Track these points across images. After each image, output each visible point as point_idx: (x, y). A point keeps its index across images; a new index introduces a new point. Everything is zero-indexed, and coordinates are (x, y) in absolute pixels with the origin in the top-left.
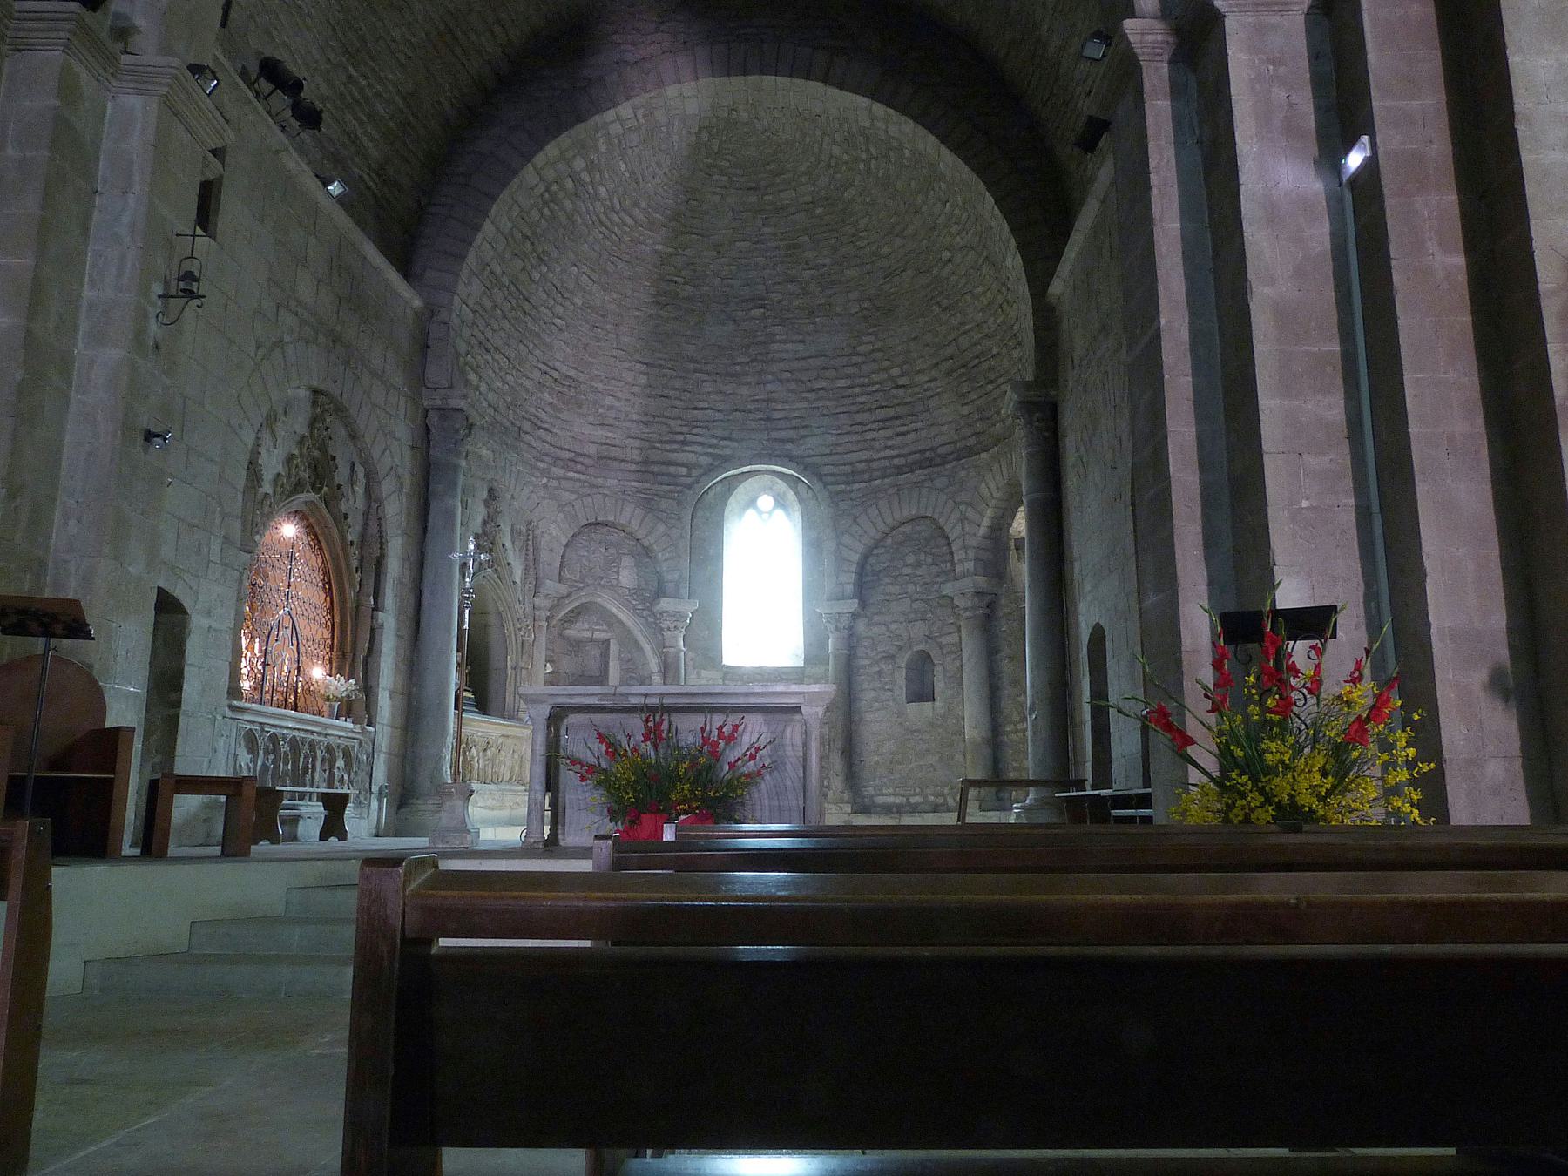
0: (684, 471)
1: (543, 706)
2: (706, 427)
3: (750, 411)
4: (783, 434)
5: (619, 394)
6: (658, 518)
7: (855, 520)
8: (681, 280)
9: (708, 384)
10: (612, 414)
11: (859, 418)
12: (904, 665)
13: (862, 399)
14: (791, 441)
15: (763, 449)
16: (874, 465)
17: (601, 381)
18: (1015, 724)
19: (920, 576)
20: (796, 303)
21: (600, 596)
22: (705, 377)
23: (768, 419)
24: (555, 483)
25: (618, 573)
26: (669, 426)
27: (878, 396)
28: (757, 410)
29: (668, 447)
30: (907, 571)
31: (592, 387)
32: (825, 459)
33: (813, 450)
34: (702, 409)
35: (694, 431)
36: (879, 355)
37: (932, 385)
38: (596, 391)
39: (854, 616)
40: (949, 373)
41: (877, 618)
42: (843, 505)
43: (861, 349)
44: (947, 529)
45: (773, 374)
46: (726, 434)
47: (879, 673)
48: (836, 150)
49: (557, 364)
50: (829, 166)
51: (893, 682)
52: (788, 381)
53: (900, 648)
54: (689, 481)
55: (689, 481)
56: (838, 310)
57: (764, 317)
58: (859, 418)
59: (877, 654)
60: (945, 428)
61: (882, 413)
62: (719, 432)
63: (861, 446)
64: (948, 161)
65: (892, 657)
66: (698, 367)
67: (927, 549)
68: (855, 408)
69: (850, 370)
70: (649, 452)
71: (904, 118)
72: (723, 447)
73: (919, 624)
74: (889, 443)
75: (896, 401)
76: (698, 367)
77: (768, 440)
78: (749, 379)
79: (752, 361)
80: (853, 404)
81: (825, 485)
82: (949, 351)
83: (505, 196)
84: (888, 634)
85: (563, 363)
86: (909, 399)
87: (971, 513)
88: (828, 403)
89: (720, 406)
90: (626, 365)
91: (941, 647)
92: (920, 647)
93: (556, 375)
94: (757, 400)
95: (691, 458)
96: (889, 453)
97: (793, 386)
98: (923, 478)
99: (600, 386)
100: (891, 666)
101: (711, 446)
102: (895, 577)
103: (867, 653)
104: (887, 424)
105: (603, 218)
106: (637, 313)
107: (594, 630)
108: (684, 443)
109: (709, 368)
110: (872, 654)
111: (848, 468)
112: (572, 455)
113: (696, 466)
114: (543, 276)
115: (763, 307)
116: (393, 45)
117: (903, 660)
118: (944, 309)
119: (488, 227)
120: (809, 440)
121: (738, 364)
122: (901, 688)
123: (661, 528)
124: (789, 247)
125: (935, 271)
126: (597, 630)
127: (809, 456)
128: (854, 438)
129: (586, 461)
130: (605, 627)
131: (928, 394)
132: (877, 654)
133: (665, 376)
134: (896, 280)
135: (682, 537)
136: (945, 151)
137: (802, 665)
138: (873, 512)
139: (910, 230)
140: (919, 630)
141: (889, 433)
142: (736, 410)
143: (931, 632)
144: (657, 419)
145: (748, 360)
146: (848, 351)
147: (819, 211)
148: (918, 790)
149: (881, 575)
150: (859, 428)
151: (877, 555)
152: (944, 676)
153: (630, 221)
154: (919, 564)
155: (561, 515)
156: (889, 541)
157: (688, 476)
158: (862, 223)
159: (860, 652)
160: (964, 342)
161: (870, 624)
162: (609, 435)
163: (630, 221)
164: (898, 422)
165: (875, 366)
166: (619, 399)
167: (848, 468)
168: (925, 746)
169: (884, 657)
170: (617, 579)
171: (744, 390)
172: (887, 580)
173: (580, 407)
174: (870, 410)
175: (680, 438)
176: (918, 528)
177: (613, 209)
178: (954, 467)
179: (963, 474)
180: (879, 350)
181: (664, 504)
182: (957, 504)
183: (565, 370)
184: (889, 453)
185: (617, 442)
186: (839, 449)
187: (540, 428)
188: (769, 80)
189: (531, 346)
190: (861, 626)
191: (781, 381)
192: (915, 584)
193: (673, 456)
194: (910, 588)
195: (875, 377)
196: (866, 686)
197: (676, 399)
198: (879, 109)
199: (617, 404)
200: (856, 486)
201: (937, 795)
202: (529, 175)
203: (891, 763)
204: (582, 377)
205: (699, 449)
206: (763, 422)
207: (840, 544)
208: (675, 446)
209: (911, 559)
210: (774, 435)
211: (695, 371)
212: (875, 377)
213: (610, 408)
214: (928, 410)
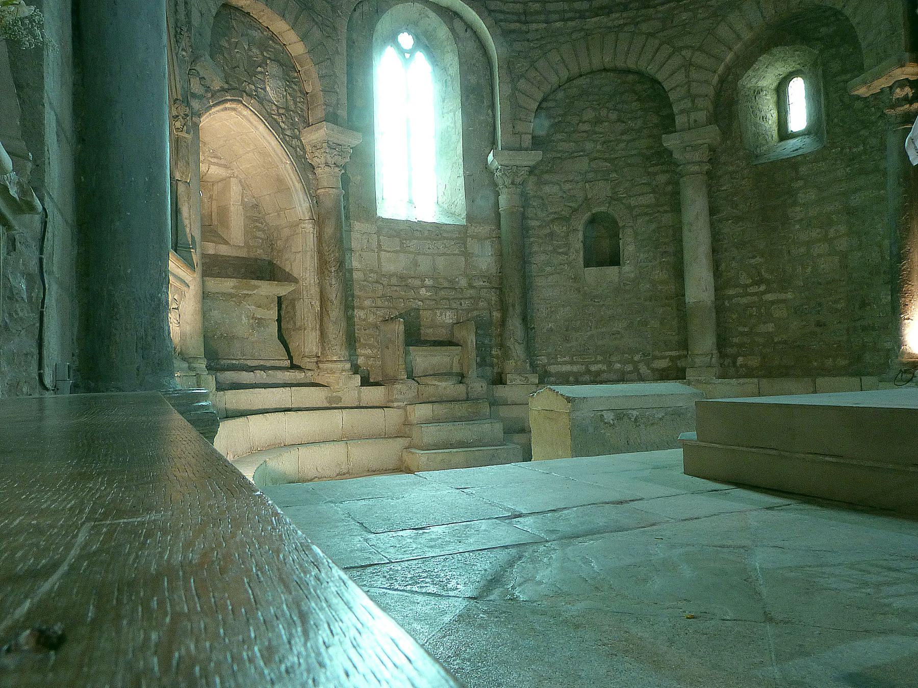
7: (532, 64)
19: (601, 133)
30: (586, 127)
41: (546, 177)
47: (552, 235)
51: (568, 245)
53: (575, 210)
59: (548, 216)
67: (610, 105)
73: (601, 184)
84: (560, 194)
91: (630, 208)
98: (621, 22)
100: (565, 228)
117: (580, 223)
126: (214, 164)
132: (548, 216)
137: (464, 222)
138: (554, 57)
140: (602, 189)
152: (635, 238)
154: (598, 121)
168: (609, 312)
170: (264, 89)
176: (596, 82)
179: (684, 16)
182: (677, 50)
194: (589, 146)
196: (535, 248)
201: (624, 362)
207: (515, 89)
209: (589, 115)
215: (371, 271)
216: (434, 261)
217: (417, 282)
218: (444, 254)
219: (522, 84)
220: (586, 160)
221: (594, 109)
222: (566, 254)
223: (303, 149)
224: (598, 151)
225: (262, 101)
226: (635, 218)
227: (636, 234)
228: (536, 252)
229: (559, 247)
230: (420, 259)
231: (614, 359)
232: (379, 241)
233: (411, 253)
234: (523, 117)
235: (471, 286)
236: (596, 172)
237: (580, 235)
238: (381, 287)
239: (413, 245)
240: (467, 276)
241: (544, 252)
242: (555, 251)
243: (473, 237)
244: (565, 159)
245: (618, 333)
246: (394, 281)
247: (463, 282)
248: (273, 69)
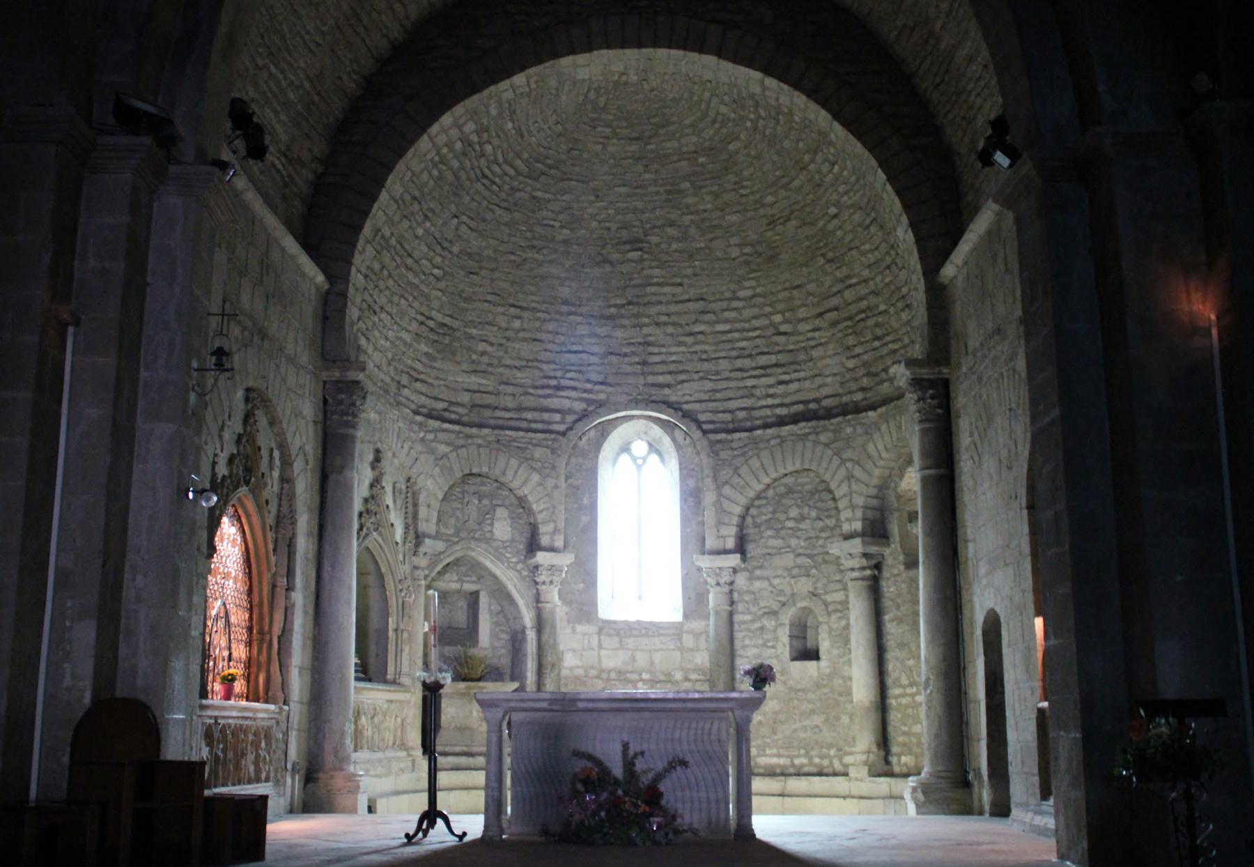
0: (557, 417)
1: (498, 709)
2: (580, 372)
3: (625, 355)
4: (660, 379)
5: (492, 339)
6: (532, 467)
8: (557, 224)
9: (583, 327)
10: (485, 359)
11: (739, 363)
12: (787, 622)
13: (743, 344)
14: (669, 386)
15: (639, 394)
16: (756, 413)
17: (475, 327)
18: (904, 687)
20: (675, 246)
21: (473, 550)
22: (579, 319)
23: (644, 363)
24: (430, 436)
25: (492, 525)
26: (541, 370)
27: (758, 342)
28: (633, 353)
29: (540, 392)
30: (790, 524)
31: (466, 333)
32: (704, 406)
33: (690, 395)
34: (576, 352)
35: (569, 375)
36: (760, 300)
37: (817, 334)
38: (471, 337)
40: (834, 324)
41: (758, 572)
42: (723, 455)
43: (741, 294)
44: (833, 486)
45: (649, 316)
46: (600, 378)
47: (762, 629)
48: (723, 109)
49: (434, 314)
50: (714, 121)
51: (776, 639)
52: (665, 324)
53: (784, 604)
54: (562, 428)
56: (719, 254)
57: (642, 260)
58: (739, 363)
60: (829, 380)
61: (763, 360)
62: (594, 377)
63: (741, 393)
64: (838, 132)
65: (773, 613)
66: (573, 309)
67: (811, 503)
68: (734, 353)
69: (732, 315)
70: (522, 398)
71: (797, 93)
72: (598, 392)
73: (804, 579)
74: (771, 391)
75: (777, 348)
76: (573, 309)
77: (645, 385)
78: (625, 322)
79: (630, 303)
80: (733, 349)
81: (705, 432)
82: (834, 302)
83: (400, 166)
84: (770, 589)
85: (439, 311)
86: (791, 347)
87: (858, 472)
88: (707, 348)
89: (595, 349)
90: (500, 309)
91: (826, 604)
92: (804, 604)
93: (431, 324)
94: (633, 344)
95: (566, 404)
96: (770, 401)
97: (670, 329)
98: (807, 431)
99: (474, 332)
101: (586, 391)
102: (778, 530)
103: (748, 609)
104: (769, 371)
105: (487, 172)
106: (513, 258)
107: (463, 582)
109: (584, 310)
110: (754, 609)
111: (728, 417)
112: (445, 405)
114: (426, 231)
115: (640, 249)
116: (307, 37)
117: (787, 617)
118: (831, 261)
119: (384, 197)
120: (686, 385)
121: (615, 306)
122: (784, 646)
123: (535, 478)
124: (669, 192)
125: (821, 223)
126: (468, 582)
127: (687, 402)
128: (733, 384)
129: (460, 410)
130: (474, 578)
131: (812, 343)
133: (538, 319)
134: (779, 228)
135: (556, 487)
136: (836, 125)
137: (678, 617)
138: (755, 463)
139: (796, 183)
141: (771, 380)
142: (611, 353)
143: (816, 588)
144: (530, 364)
145: (624, 302)
146: (728, 295)
147: (701, 160)
148: (802, 752)
149: (763, 528)
150: (739, 374)
151: (759, 507)
153: (511, 172)
154: (802, 518)
155: (437, 470)
156: (771, 493)
157: (562, 422)
158: (746, 173)
160: (849, 295)
161: (752, 578)
162: (483, 381)
163: (511, 172)
164: (779, 370)
165: (756, 311)
166: (492, 344)
167: (728, 417)
168: (810, 706)
169: (766, 613)
170: (491, 531)
171: (619, 333)
172: (769, 533)
173: (454, 354)
174: (750, 356)
175: (553, 382)
176: (800, 481)
177: (496, 162)
178: (840, 423)
179: (849, 430)
180: (759, 295)
181: (538, 453)
182: (843, 462)
183: (439, 317)
184: (770, 401)
185: (490, 389)
186: (718, 396)
187: (417, 380)
188: (662, 52)
189: (411, 299)
191: (657, 324)
192: (798, 538)
194: (794, 542)
195: (756, 323)
197: (549, 342)
198: (772, 83)
199: (489, 349)
200: (737, 435)
201: (822, 757)
202: (424, 143)
203: (774, 722)
204: (456, 324)
205: (573, 394)
206: (639, 367)
207: (720, 495)
208: (548, 391)
209: (794, 512)
210: (651, 379)
211: (571, 313)
212: (756, 323)
213: (483, 353)
214: (811, 360)
215: (592, 667)
216: (651, 658)
217: (635, 677)
218: (661, 650)
219: (727, 490)
220: (792, 556)
221: (798, 506)
222: (773, 647)
224: (802, 547)
226: (829, 614)
227: (831, 629)
228: (747, 646)
229: (768, 641)
230: (639, 655)
231: (814, 753)
232: (600, 640)
233: (628, 649)
234: (726, 521)
235: (687, 679)
236: (799, 567)
237: (787, 630)
238: (600, 682)
239: (631, 642)
240: (682, 669)
241: (755, 646)
242: (764, 645)
243: (688, 632)
244: (775, 554)
245: (817, 726)
246: (613, 675)
247: (678, 676)
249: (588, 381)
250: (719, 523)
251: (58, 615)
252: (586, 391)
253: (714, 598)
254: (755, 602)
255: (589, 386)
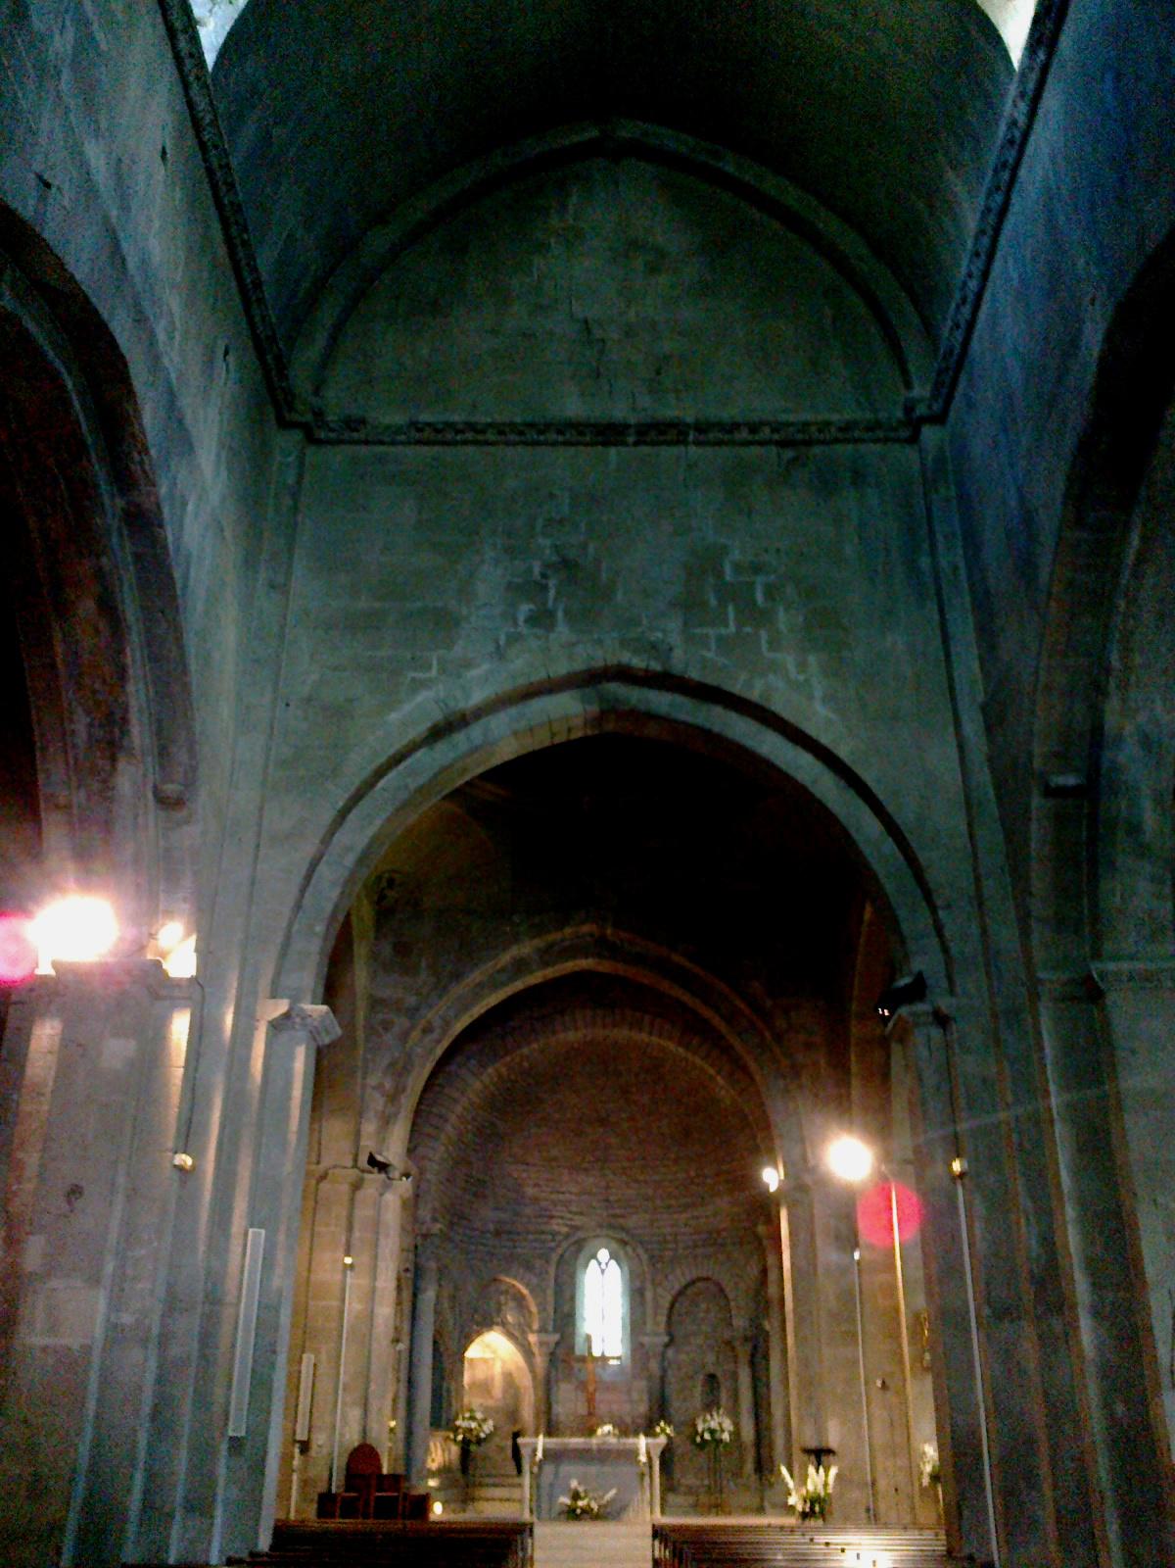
14: (623, 1216)
39: (667, 1346)
54: (553, 1244)
55: (553, 1244)
62: (574, 1209)
89: (574, 1190)
101: (571, 1219)
108: (552, 1217)
113: (559, 1233)
157: (553, 1240)
159: (670, 1372)
190: (670, 1353)
193: (543, 1228)
205: (560, 1221)
209: (703, 1306)
219: (660, 1290)
220: (702, 1337)
223: (529, 1344)
225: (504, 1324)
248: (512, 1304)
249: (570, 1212)
250: (656, 1314)
251: (344, 1404)
252: (571, 1219)
253: (654, 1366)
254: (679, 1369)
255: (569, 1216)
